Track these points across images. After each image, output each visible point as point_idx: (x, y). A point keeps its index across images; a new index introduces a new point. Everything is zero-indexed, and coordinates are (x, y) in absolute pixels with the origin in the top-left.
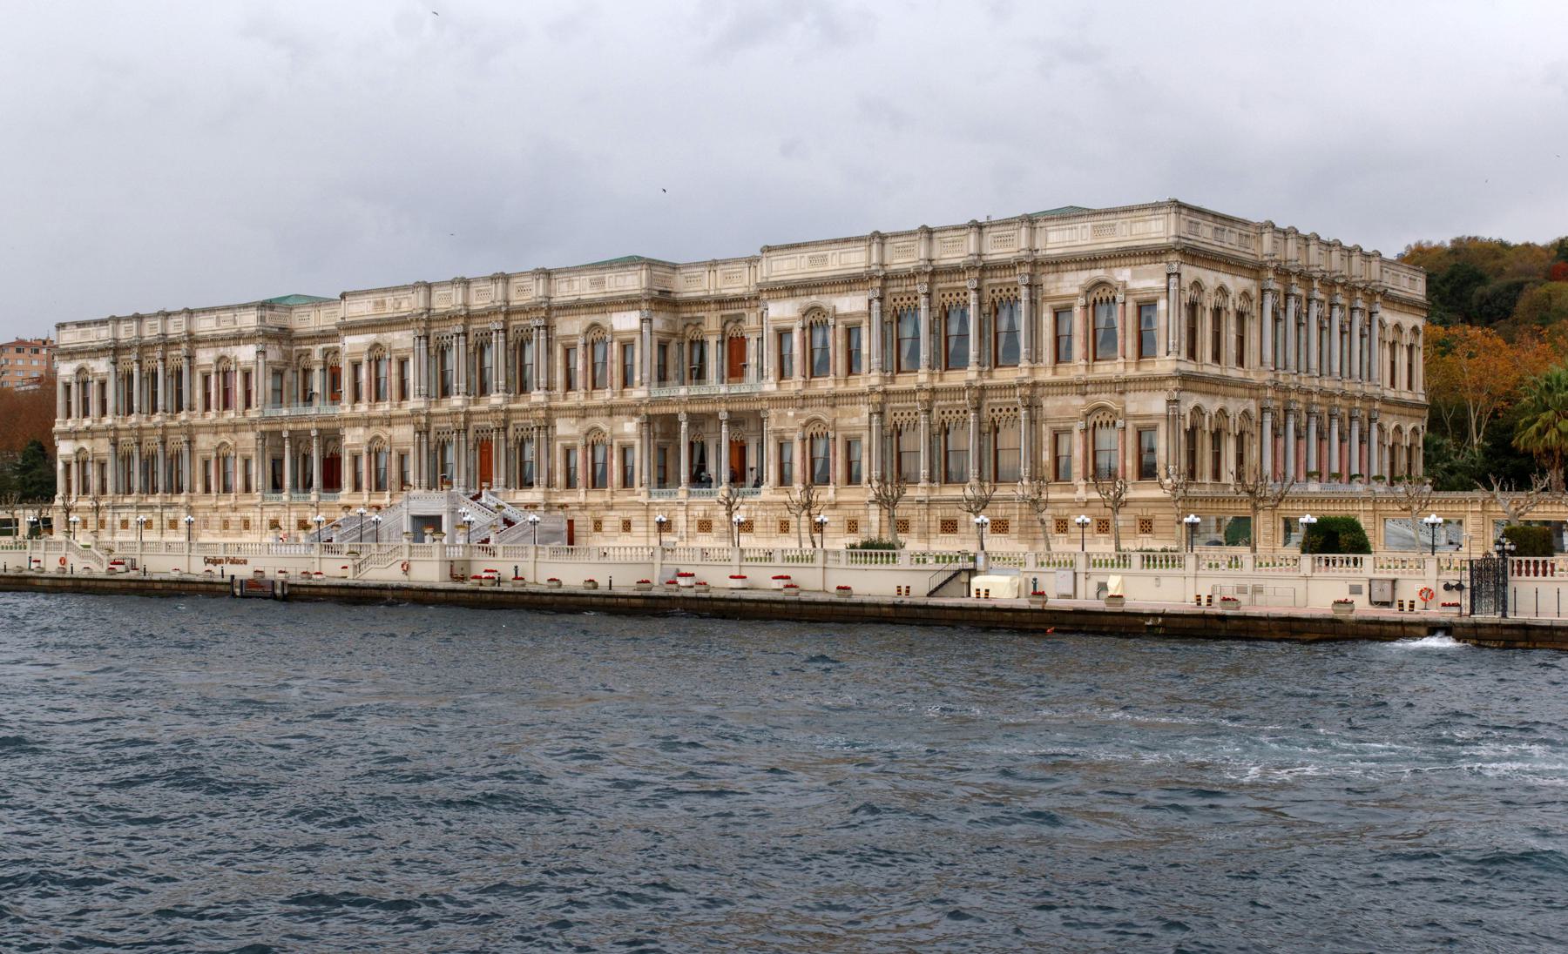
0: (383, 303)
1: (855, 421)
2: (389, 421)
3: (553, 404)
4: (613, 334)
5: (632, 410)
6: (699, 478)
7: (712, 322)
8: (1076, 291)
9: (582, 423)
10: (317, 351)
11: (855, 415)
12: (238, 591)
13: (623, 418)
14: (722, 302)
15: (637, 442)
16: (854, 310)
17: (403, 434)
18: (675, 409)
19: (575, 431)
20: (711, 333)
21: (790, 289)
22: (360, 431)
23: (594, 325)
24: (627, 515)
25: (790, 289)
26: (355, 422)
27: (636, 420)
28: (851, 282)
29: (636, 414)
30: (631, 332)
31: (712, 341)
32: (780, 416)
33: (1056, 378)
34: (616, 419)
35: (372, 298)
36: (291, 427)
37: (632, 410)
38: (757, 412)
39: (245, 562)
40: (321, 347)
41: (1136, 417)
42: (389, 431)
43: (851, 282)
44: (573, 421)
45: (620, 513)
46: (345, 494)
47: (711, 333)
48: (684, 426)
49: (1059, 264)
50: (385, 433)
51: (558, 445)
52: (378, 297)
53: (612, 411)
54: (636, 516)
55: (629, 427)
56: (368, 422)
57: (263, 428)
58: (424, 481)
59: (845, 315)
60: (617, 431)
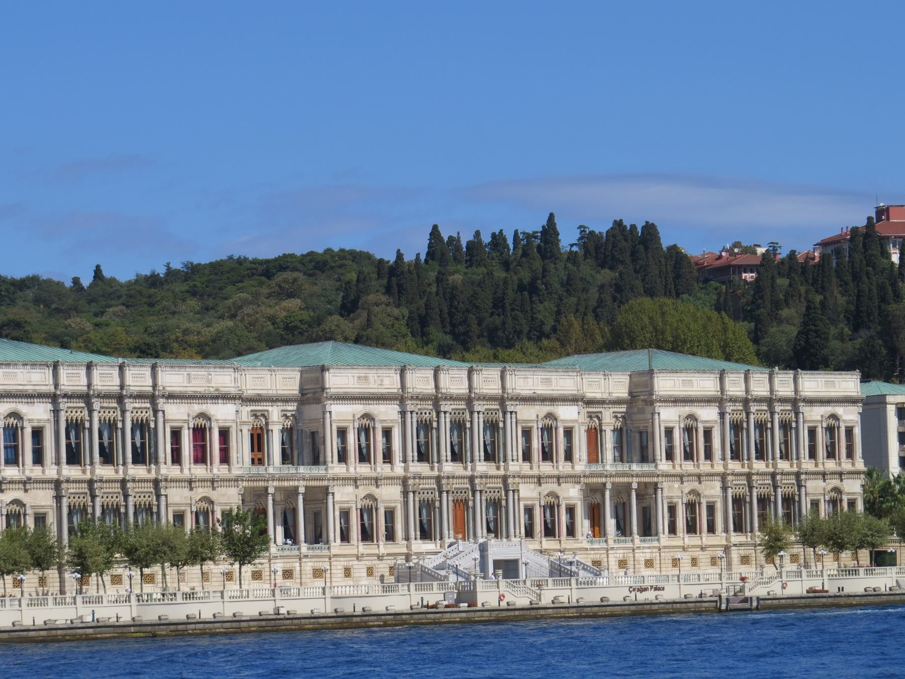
1: (712, 492)
2: (376, 481)
5: (574, 478)
6: (647, 530)
8: (819, 418)
11: (713, 488)
12: (724, 607)
13: (569, 485)
16: (709, 419)
18: (604, 480)
21: (677, 401)
22: (350, 489)
25: (677, 401)
27: (578, 487)
28: (707, 401)
32: (670, 487)
33: (817, 469)
36: (276, 483)
37: (574, 478)
38: (656, 484)
39: (663, 589)
41: (849, 494)
43: (707, 401)
44: (532, 486)
46: (665, 539)
49: (811, 402)
57: (245, 484)
59: (705, 422)
60: (565, 496)
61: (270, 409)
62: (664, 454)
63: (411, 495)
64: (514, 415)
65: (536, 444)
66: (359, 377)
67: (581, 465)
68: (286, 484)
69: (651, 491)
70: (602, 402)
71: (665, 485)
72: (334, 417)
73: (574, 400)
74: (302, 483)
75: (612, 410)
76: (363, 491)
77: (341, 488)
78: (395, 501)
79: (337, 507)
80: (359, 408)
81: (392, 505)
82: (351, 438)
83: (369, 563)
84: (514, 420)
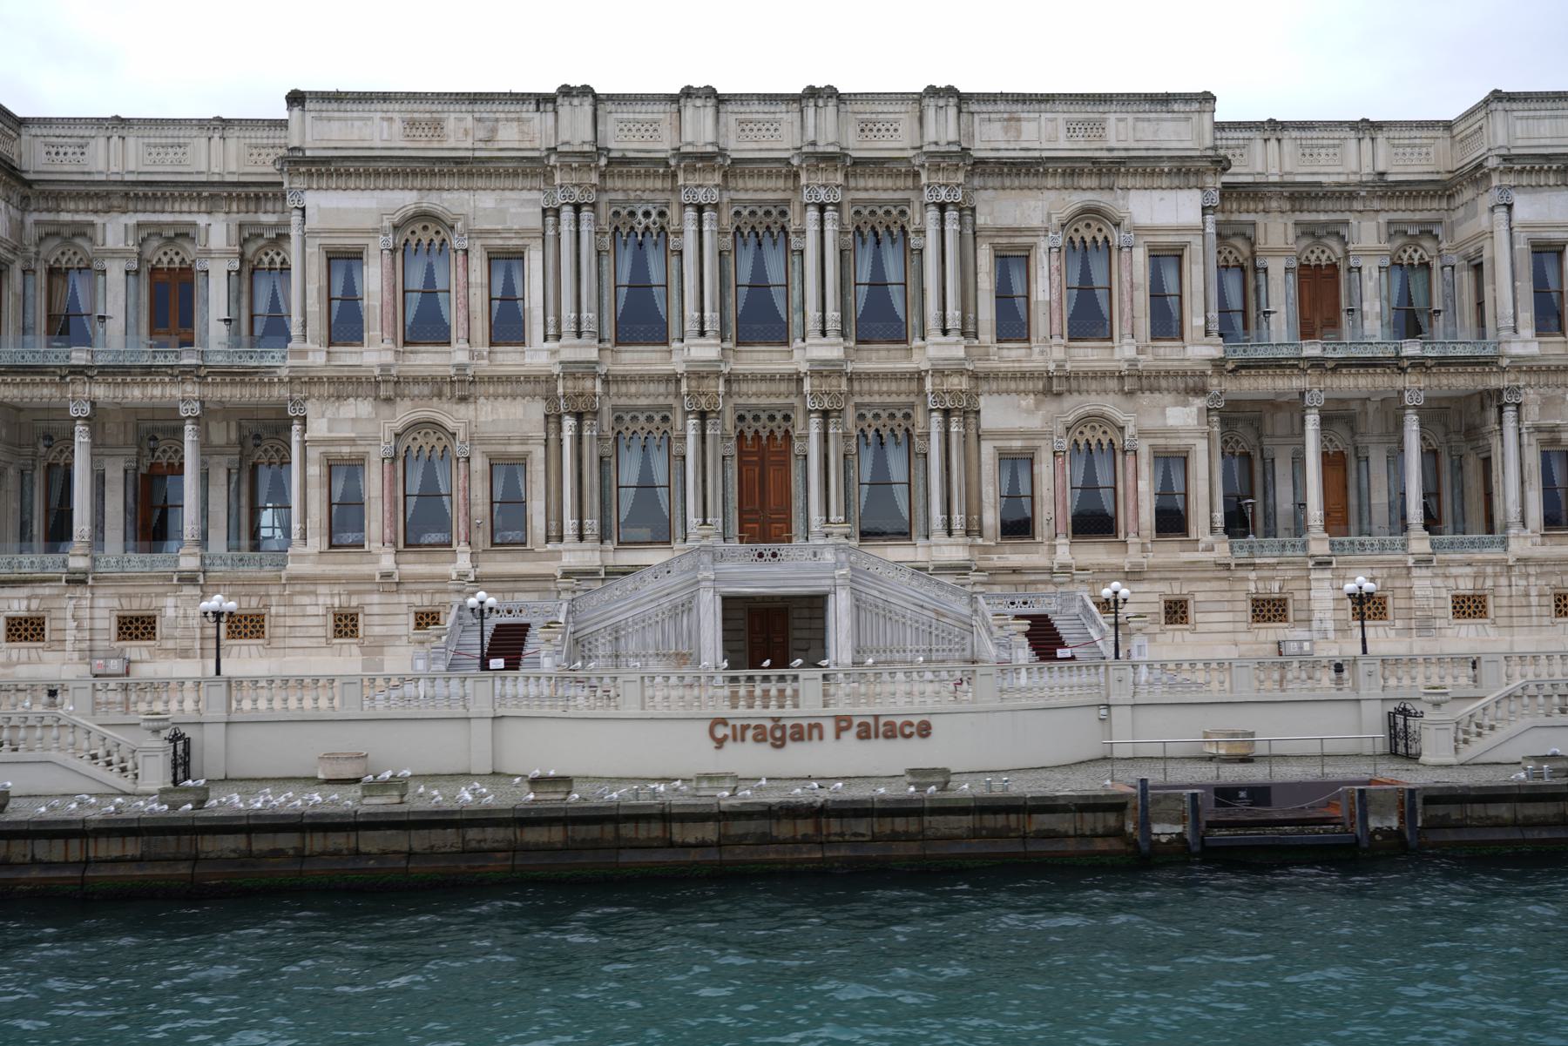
0: (437, 125)
2: (463, 387)
3: (981, 366)
4: (1138, 230)
7: (1277, 233)
9: (1051, 406)
10: (115, 230)
13: (1168, 398)
14: (1300, 195)
15: (1201, 446)
17: (514, 420)
19: (1035, 422)
20: (1274, 252)
22: (362, 408)
23: (1090, 213)
24: (1176, 590)
26: (346, 385)
27: (1200, 402)
29: (1201, 391)
30: (1178, 230)
31: (1276, 267)
32: (1546, 403)
34: (1145, 399)
35: (397, 110)
36: (100, 392)
40: (132, 219)
42: (465, 411)
44: (1031, 399)
45: (1164, 588)
47: (1274, 252)
48: (1312, 421)
50: (454, 416)
51: (988, 450)
52: (421, 112)
53: (1137, 382)
54: (1199, 593)
55: (1182, 419)
56: (385, 388)
58: (592, 524)
60: (1149, 423)
61: (202, 220)
62: (1527, 316)
63: (569, 422)
64: (951, 215)
65: (1046, 287)
66: (412, 124)
67: (1199, 349)
68: (135, 394)
69: (1492, 414)
70: (1345, 194)
71: (1530, 396)
72: (312, 223)
73: (1183, 170)
74: (192, 390)
75: (1383, 218)
76: (405, 413)
77: (330, 409)
78: (525, 440)
79: (314, 453)
80: (404, 199)
81: (515, 449)
82: (374, 280)
83: (423, 601)
84: (952, 227)
